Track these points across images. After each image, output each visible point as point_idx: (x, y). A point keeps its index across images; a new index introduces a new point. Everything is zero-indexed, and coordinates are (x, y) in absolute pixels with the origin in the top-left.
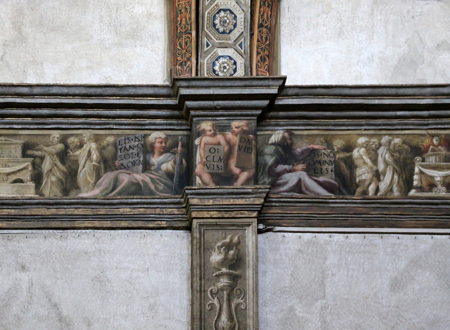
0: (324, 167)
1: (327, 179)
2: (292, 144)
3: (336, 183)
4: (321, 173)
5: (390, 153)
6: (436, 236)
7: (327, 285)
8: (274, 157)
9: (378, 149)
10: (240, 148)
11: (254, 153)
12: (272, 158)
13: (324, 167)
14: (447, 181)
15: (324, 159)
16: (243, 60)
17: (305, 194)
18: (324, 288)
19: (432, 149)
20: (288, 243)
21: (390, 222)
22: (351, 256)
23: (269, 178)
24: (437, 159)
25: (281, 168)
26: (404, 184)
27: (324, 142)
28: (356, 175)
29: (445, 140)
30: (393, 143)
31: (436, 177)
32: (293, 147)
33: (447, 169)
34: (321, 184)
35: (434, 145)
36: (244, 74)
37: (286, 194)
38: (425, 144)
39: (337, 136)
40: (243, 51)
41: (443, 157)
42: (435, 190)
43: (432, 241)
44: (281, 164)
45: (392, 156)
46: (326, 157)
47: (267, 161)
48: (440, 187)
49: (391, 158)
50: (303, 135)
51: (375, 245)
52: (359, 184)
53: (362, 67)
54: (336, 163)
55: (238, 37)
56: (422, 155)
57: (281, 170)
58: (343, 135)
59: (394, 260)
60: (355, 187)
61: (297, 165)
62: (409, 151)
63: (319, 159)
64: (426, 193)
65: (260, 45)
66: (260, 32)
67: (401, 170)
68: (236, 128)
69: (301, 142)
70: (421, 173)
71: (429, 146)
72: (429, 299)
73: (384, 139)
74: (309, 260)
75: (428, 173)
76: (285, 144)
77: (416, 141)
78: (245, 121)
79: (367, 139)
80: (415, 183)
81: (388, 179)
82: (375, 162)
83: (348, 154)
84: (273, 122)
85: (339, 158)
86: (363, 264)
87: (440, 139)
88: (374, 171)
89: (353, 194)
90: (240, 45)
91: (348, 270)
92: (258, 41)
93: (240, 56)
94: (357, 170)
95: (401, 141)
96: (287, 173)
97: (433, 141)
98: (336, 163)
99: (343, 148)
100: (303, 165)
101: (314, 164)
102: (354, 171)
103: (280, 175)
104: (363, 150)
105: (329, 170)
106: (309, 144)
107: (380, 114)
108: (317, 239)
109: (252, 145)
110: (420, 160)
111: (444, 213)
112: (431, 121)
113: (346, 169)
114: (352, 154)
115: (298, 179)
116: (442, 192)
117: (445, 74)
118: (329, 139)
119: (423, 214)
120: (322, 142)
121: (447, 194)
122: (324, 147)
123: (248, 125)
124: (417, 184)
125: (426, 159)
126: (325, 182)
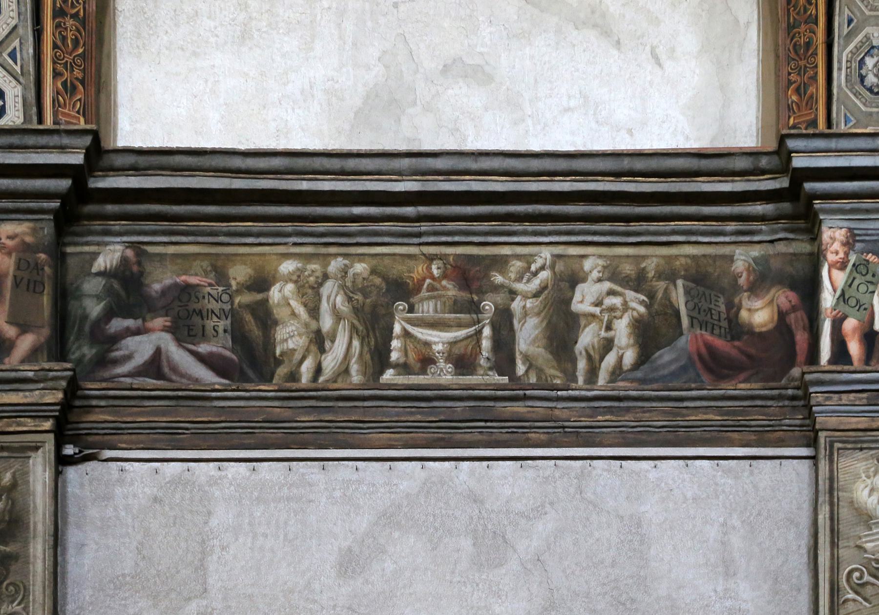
0: (210, 324)
1: (214, 349)
2: (141, 273)
3: (234, 357)
4: (203, 335)
5: (345, 293)
6: (431, 463)
7: (211, 568)
8: (104, 302)
9: (321, 285)
10: (18, 283)
11: (48, 294)
12: (98, 304)
13: (210, 324)
14: (457, 352)
15: (210, 307)
16: (19, 88)
17: (170, 380)
18: (205, 574)
19: (428, 285)
20: (132, 484)
21: (340, 437)
22: (262, 507)
23: (91, 347)
24: (439, 306)
25: (117, 324)
26: (372, 358)
27: (210, 271)
28: (275, 339)
29: (455, 267)
30: (351, 272)
31: (435, 343)
32: (142, 279)
33: (457, 326)
34: (204, 359)
35: (433, 278)
36: (22, 120)
37: (128, 380)
38: (415, 276)
39: (239, 258)
40: (18, 69)
41: (449, 303)
42: (432, 370)
43: (423, 474)
44: (118, 316)
45: (350, 299)
46: (214, 301)
47: (88, 311)
48: (441, 364)
49: (346, 303)
50: (166, 254)
51: (311, 485)
52: (281, 358)
53: (290, 111)
54: (234, 315)
55: (7, 36)
56: (409, 298)
57: (119, 329)
58: (249, 254)
59: (348, 514)
60: (273, 365)
61: (152, 319)
62: (384, 291)
63: (197, 306)
64: (413, 377)
65: (60, 56)
66: (58, 26)
67: (367, 329)
68: (9, 237)
69: (161, 270)
70: (406, 334)
71: (424, 280)
72: (411, 591)
73: (335, 265)
74: (175, 517)
75: (419, 336)
76: (127, 273)
77: (397, 269)
78: (31, 225)
79: (300, 265)
80: (394, 356)
81: (340, 347)
82: (314, 312)
83: (259, 297)
84: (97, 225)
85: (240, 305)
86: (286, 523)
87: (445, 264)
88: (312, 332)
89: (269, 379)
90: (12, 56)
91: (255, 537)
92: (55, 46)
93: (11, 79)
94: (278, 328)
95: (369, 270)
96: (130, 336)
97: (431, 268)
98: (234, 315)
99: (248, 283)
100: (166, 318)
101: (188, 318)
102: (272, 332)
103: (115, 339)
104: (290, 287)
105: (220, 330)
106: (179, 275)
107: (318, 212)
108: (193, 474)
109: (43, 275)
110: (404, 309)
111: (442, 418)
112: (425, 227)
113: (255, 328)
114: (268, 296)
115: (154, 349)
116: (445, 375)
117: (457, 130)
118: (219, 264)
119: (403, 419)
120: (205, 271)
121: (455, 377)
122: (210, 281)
123: (34, 231)
124: (398, 359)
125: (416, 306)
126: (211, 354)
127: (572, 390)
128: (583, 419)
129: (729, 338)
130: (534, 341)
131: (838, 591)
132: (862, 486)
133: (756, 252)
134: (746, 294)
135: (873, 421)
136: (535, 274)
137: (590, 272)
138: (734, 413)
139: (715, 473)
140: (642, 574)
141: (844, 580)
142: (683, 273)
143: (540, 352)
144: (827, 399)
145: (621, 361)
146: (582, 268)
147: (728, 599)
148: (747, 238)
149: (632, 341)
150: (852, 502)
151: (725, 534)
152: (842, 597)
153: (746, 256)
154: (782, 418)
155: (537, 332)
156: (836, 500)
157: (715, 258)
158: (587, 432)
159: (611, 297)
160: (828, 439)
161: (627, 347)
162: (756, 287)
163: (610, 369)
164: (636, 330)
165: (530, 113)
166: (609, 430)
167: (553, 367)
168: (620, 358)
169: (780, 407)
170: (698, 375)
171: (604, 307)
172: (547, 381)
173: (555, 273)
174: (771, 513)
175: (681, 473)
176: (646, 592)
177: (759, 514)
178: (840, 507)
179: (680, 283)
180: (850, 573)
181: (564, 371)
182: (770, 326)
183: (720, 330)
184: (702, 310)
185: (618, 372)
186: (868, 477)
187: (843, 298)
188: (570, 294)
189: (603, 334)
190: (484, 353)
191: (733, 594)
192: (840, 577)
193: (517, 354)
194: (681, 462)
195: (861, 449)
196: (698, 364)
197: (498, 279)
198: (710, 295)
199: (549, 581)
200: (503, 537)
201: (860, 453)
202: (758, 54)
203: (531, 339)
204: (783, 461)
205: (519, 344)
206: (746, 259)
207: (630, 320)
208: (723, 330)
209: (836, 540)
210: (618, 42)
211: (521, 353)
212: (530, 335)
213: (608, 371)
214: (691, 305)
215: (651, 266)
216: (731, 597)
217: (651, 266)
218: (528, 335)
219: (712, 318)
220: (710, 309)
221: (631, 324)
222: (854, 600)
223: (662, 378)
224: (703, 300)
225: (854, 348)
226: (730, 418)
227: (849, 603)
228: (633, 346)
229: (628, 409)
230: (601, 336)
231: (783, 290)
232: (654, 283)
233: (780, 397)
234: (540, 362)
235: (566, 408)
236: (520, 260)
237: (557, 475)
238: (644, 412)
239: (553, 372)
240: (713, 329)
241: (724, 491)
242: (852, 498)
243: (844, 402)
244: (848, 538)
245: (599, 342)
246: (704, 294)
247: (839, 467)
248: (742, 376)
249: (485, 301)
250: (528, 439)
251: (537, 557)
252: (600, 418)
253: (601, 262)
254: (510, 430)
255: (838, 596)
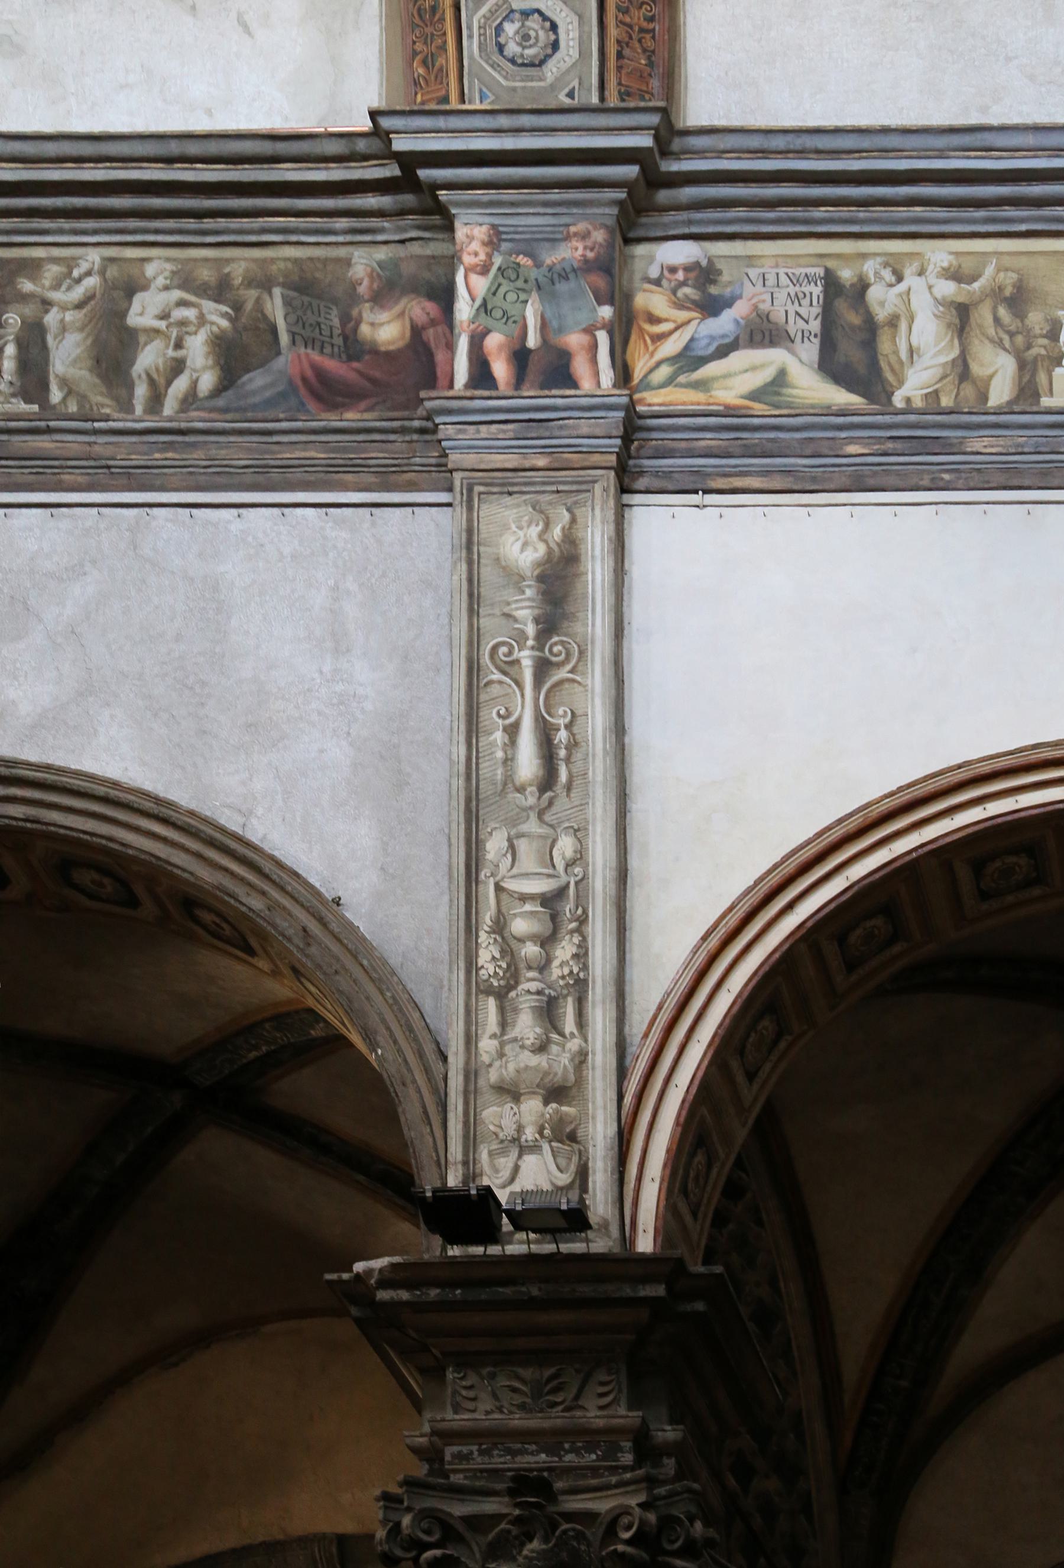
127: (114, 420)
128: (133, 457)
129: (344, 356)
130: (74, 362)
131: (478, 670)
132: (512, 539)
133: (382, 254)
134: (367, 305)
135: (525, 458)
136: (78, 281)
137: (154, 278)
138: (345, 450)
139: (323, 524)
140: (217, 650)
141: (487, 656)
142: (281, 280)
143: (83, 376)
144: (460, 431)
145: (196, 386)
146: (143, 273)
147: (338, 682)
148: (368, 238)
149: (210, 362)
150: (498, 559)
151: (336, 600)
152: (483, 679)
153: (367, 259)
154: (411, 455)
155: (78, 351)
156: (476, 557)
157: (325, 261)
158: (142, 473)
159: (182, 308)
160: (465, 481)
161: (205, 368)
162: (380, 298)
163: (180, 396)
164: (217, 349)
165: (73, 91)
166: (172, 470)
167: (102, 394)
168: (195, 384)
169: (408, 442)
170: (303, 404)
171: (172, 320)
172: (92, 409)
173: (105, 280)
174: (400, 574)
175: (275, 524)
176: (223, 673)
177: (384, 575)
178: (481, 565)
179: (277, 291)
180: (495, 649)
181: (116, 399)
182: (400, 344)
183: (333, 348)
184: (307, 325)
185: (190, 399)
186: (520, 528)
187: (485, 307)
188: (125, 305)
189: (171, 353)
190: (5, 376)
191: (345, 676)
192: (481, 653)
193: (52, 378)
194: (276, 511)
195: (510, 494)
196: (303, 391)
197: (27, 286)
198: (319, 306)
199: (86, 658)
200: (25, 603)
201: (510, 498)
202: (381, 20)
203: (70, 359)
204: (416, 509)
205: (53, 366)
206: (368, 262)
207: (208, 336)
208: (336, 349)
209: (476, 607)
210: (193, 8)
211: (57, 376)
212: (69, 354)
213: (177, 398)
214: (292, 318)
215: (237, 271)
216: (342, 680)
217: (237, 271)
218: (67, 354)
219: (321, 334)
220: (319, 324)
221: (209, 341)
222: (500, 682)
223: (254, 407)
224: (309, 312)
225: (501, 369)
226: (338, 456)
227: (493, 685)
228: (212, 368)
229: (194, 445)
230: (168, 356)
231: (417, 300)
232: (242, 292)
233: (403, 431)
234: (83, 387)
235: (110, 443)
236: (59, 264)
237: (102, 526)
238: (222, 448)
239: (100, 399)
240: (322, 347)
241: (335, 547)
242: (498, 554)
243: (483, 435)
244: (492, 605)
245: (165, 363)
246: (310, 304)
247: (481, 515)
248: (363, 405)
249: (8, 312)
250: (61, 481)
251: (71, 629)
252: (157, 456)
253: (169, 267)
254: (34, 470)
255: (478, 676)
